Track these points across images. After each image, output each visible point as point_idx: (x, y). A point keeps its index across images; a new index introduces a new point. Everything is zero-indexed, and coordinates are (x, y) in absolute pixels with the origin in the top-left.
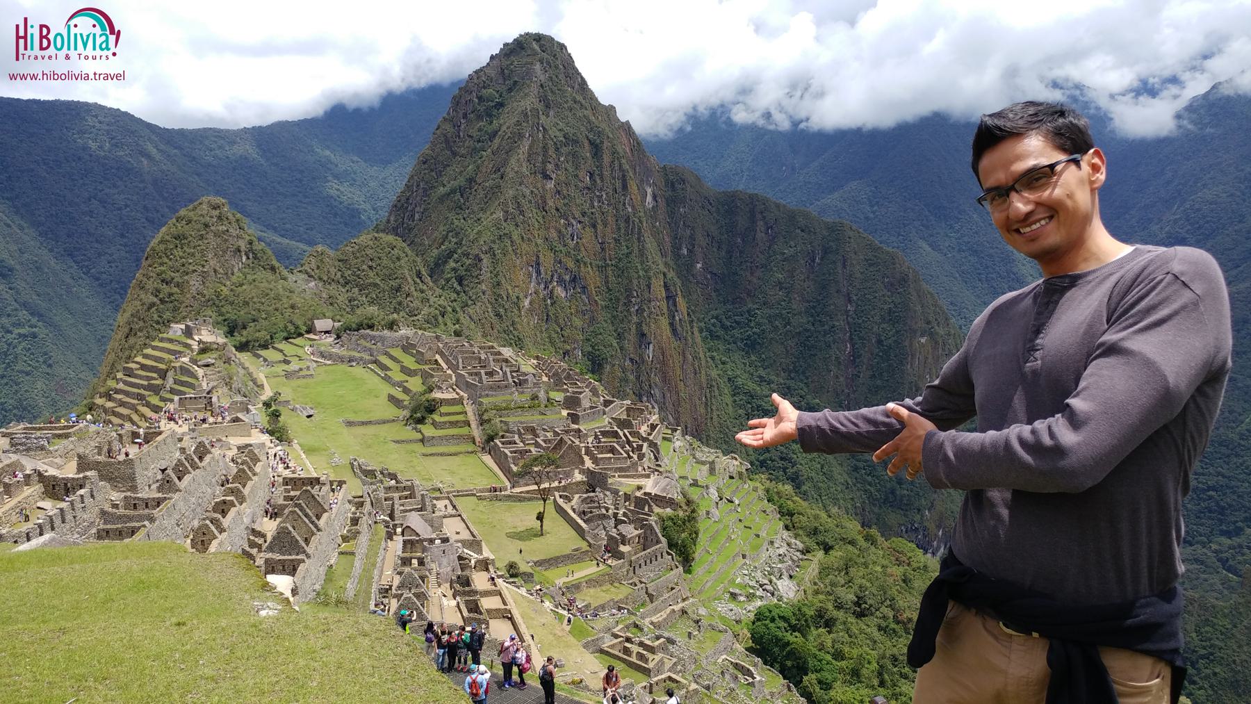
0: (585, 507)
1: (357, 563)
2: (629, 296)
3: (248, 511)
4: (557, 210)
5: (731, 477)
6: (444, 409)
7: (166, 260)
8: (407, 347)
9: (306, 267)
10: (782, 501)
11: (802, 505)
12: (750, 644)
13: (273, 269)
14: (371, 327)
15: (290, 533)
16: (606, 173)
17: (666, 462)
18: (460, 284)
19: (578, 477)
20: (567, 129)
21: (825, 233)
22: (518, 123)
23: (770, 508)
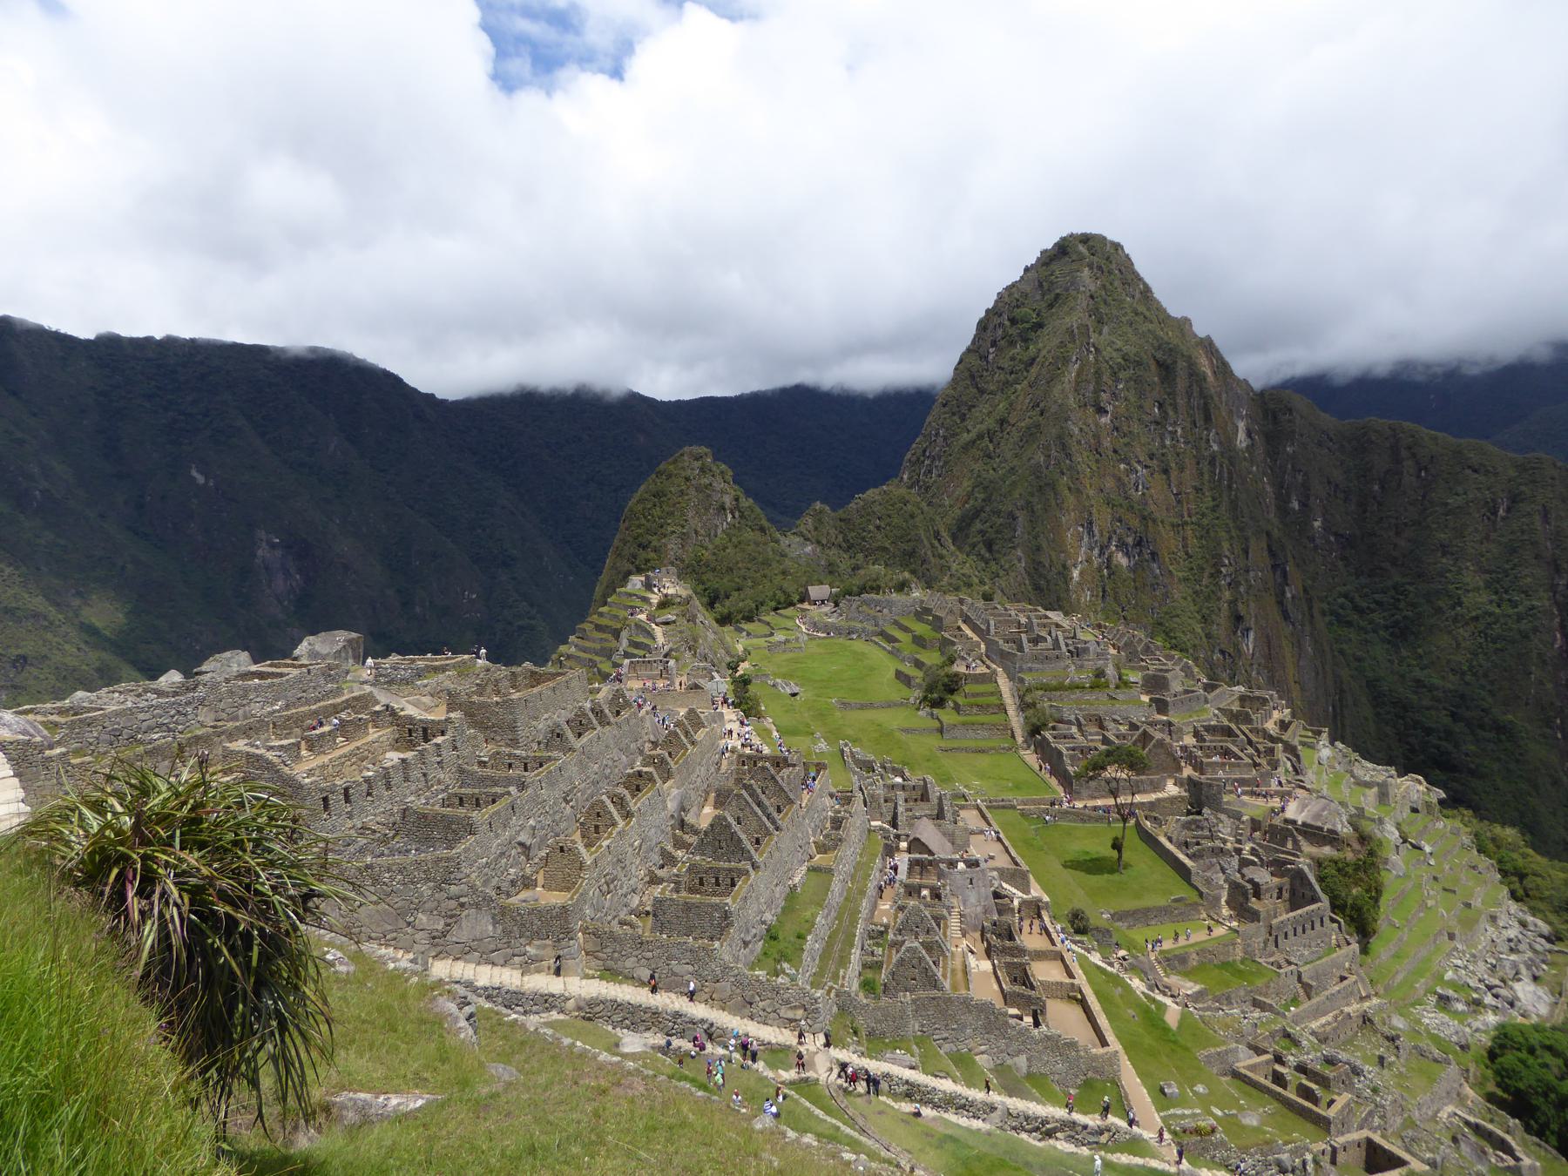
0: (1186, 835)
1: (836, 886)
2: (1217, 566)
3: (675, 792)
4: (1115, 451)
5: (1414, 810)
6: (967, 689)
7: (643, 521)
8: (922, 613)
9: (802, 528)
10: (1503, 852)
11: (1538, 862)
12: (1491, 1087)
13: (762, 529)
14: (877, 589)
15: (729, 826)
16: (1181, 401)
17: (1310, 778)
18: (990, 550)
19: (1172, 789)
20: (1126, 349)
21: (1512, 473)
22: (1062, 344)
23: (1484, 862)
